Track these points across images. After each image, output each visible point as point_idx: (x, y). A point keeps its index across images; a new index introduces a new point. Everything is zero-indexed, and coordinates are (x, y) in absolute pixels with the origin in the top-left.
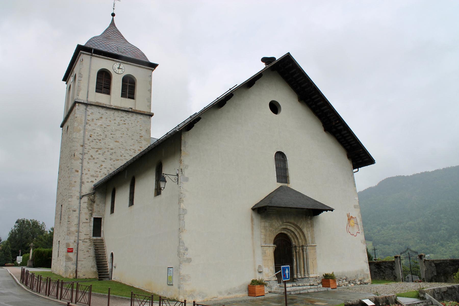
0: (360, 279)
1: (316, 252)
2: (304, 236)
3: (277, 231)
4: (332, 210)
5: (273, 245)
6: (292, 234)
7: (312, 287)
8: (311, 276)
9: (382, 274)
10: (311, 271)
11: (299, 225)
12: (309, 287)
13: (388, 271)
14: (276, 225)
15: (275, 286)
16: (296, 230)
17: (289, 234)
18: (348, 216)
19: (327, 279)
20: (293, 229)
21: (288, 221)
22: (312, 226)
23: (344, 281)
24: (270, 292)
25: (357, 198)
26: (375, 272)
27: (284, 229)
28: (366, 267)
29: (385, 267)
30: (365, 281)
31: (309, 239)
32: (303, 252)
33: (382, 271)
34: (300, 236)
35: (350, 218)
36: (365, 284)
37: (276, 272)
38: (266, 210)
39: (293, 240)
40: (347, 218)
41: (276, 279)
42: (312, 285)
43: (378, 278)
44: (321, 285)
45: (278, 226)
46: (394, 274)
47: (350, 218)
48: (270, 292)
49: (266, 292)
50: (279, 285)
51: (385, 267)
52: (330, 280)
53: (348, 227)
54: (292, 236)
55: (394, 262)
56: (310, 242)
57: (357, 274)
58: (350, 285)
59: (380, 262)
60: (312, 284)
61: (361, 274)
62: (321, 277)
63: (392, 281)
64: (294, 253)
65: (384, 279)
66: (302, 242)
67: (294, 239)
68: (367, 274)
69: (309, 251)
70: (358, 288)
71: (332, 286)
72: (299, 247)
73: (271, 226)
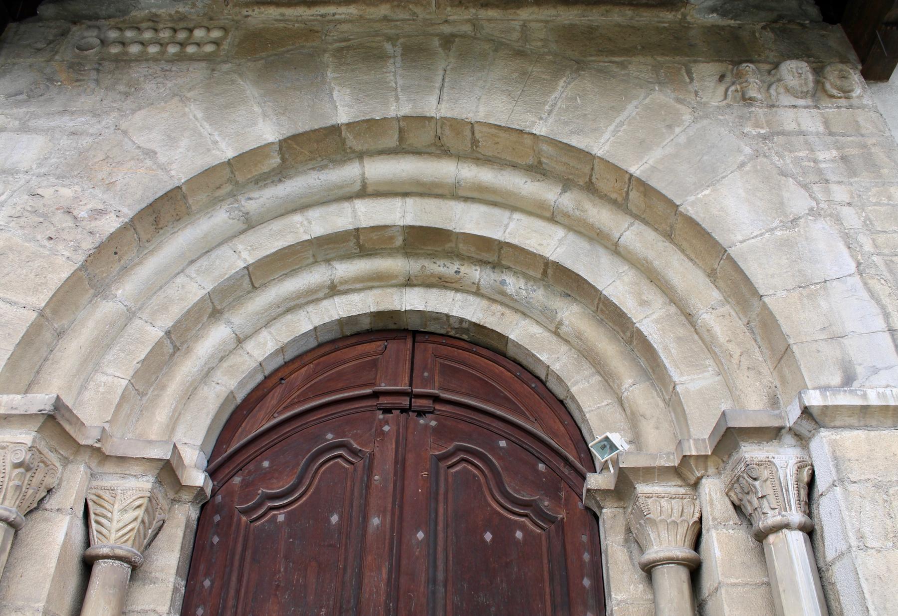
2: (739, 288)
6: (571, 314)
16: (616, 249)
17: (520, 331)
20: (551, 243)
54: (589, 356)
67: (608, 380)
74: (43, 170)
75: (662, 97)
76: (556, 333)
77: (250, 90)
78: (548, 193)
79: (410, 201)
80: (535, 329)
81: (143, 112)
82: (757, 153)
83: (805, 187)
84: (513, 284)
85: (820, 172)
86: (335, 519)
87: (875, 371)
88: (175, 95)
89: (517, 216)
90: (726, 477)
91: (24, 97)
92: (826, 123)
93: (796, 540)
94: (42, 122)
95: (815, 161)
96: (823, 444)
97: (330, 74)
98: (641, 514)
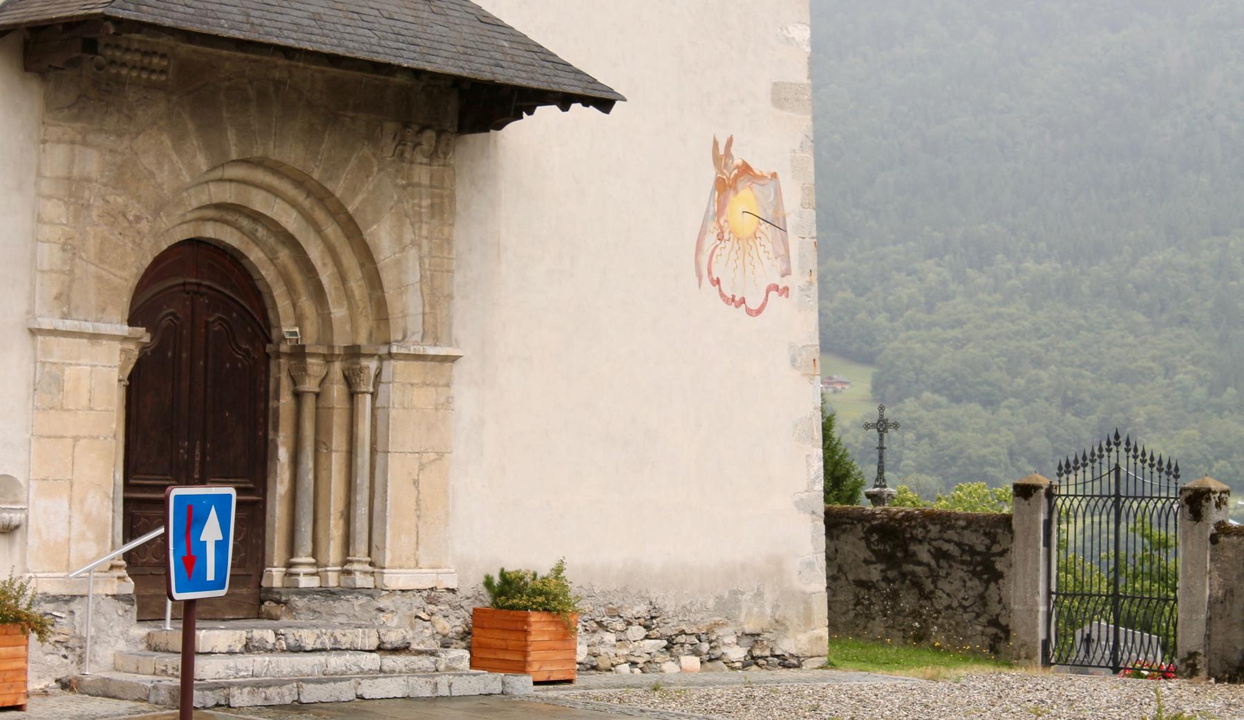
0: (749, 629)
1: (449, 400)
2: (374, 280)
3: (164, 222)
4: (605, 103)
5: (125, 329)
6: (284, 255)
7: (391, 661)
8: (395, 579)
9: (908, 601)
10: (395, 542)
11: (338, 189)
12: (372, 661)
13: (956, 586)
14: (163, 176)
15: (117, 642)
17: (255, 255)
18: (717, 159)
19: (511, 613)
20: (290, 221)
21: (257, 152)
22: (442, 207)
23: (637, 632)
24: (65, 685)
25: (802, 34)
26: (861, 584)
27: (225, 211)
28: (805, 544)
29: (940, 555)
30: (787, 646)
31: (408, 305)
32: (352, 395)
33: (917, 585)
34: (343, 278)
35: (732, 176)
36: (784, 662)
37: (129, 534)
38: (91, 46)
39: (283, 304)
40: (711, 174)
41: (129, 587)
42: (395, 650)
43: (878, 626)
44: (460, 655)
45: (176, 184)
46: (995, 608)
47: (732, 176)
48: (65, 685)
49: (34, 685)
50: (141, 631)
51: (940, 555)
52: (534, 617)
53: (710, 240)
55: (1006, 520)
56: (415, 324)
57: (735, 593)
58: (670, 667)
59: (909, 517)
60: (393, 638)
61: (759, 595)
62: (466, 590)
63: (975, 656)
64: (285, 401)
65: (921, 637)
66: (352, 319)
68: (806, 599)
69: (403, 393)
70: (724, 685)
71: (543, 662)
72: (328, 359)
73: (122, 176)
74: (104, 180)
75: (367, 151)
76: (271, 260)
77: (191, 126)
78: (301, 198)
79: (233, 185)
80: (261, 255)
81: (141, 137)
82: (400, 201)
83: (412, 224)
84: (261, 232)
85: (420, 214)
86: (170, 354)
87: (414, 334)
88: (154, 123)
89: (278, 200)
90: (347, 365)
91: (75, 111)
92: (431, 178)
93: (368, 397)
94: (90, 137)
95: (420, 207)
96: (389, 366)
97: (225, 115)
98: (305, 370)
